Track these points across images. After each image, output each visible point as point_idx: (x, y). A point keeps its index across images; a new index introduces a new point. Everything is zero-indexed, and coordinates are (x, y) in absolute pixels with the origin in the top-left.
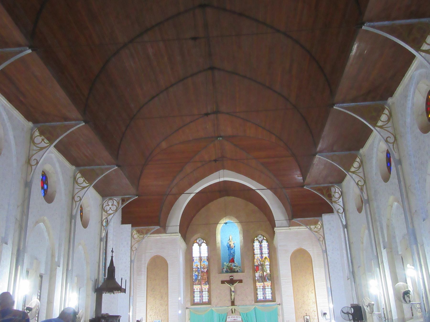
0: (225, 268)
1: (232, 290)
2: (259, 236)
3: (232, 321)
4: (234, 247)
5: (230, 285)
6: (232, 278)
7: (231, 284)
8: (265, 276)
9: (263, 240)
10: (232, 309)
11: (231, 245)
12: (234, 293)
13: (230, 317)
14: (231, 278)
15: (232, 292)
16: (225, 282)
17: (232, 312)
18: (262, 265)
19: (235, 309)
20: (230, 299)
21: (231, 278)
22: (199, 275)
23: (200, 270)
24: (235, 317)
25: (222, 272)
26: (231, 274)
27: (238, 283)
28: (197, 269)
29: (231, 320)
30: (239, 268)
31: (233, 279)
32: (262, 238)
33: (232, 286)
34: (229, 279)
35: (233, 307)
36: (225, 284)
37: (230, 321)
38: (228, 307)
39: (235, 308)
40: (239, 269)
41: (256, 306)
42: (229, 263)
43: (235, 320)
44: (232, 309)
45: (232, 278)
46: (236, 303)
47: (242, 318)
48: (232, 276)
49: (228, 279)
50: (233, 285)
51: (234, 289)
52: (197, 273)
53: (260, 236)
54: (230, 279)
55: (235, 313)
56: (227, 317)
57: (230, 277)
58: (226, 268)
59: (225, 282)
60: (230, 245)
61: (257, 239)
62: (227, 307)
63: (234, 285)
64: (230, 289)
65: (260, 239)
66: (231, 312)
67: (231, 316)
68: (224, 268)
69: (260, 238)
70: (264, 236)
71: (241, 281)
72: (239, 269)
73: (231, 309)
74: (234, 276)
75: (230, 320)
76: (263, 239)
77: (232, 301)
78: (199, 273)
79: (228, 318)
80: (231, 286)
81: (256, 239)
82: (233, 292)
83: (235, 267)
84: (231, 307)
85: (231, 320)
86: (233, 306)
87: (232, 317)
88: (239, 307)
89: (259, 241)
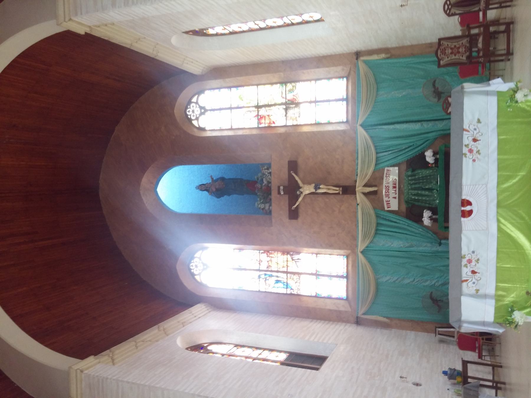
0: (263, 207)
1: (314, 191)
2: (190, 115)
3: (397, 196)
4: (222, 179)
5: (299, 196)
6: (282, 188)
7: (298, 192)
8: (284, 101)
9: (199, 105)
10: (365, 194)
11: (217, 187)
12: (321, 184)
13: (385, 199)
14: (282, 193)
15: (320, 191)
16: (293, 209)
17: (375, 193)
18: (258, 107)
19: (366, 185)
20: (338, 197)
21: (282, 193)
22: (277, 277)
23: (264, 273)
24: (387, 185)
25: (270, 213)
26: (274, 193)
27: (296, 174)
28: (262, 281)
29: (395, 198)
30: (264, 168)
31: (285, 187)
32: (193, 106)
33: (301, 190)
34: (287, 197)
35: (359, 189)
36: (300, 211)
37: (397, 200)
38: (358, 204)
39: (364, 183)
40: (265, 169)
41: (360, 122)
42: (256, 194)
43: (395, 187)
44: (365, 194)
45: (282, 188)
46: (347, 183)
47: (391, 166)
48: (279, 187)
49: (285, 201)
50: (300, 188)
51: (309, 183)
52: (272, 280)
53: (189, 111)
54: (284, 194)
55: (375, 186)
56: (386, 209)
57: (279, 193)
58: (262, 203)
59: (293, 209)
60: (217, 190)
61: (197, 119)
62: (359, 208)
63: (301, 184)
64: (323, 196)
65: (197, 111)
66: (372, 197)
67: (384, 196)
68: (263, 209)
69: (193, 111)
70: (190, 102)
71: (293, 166)
72: (265, 169)
73: (362, 196)
74: (279, 185)
75: (394, 199)
76: (197, 103)
77: (341, 194)
78: (271, 276)
79: (388, 208)
80: (302, 193)
81: (195, 123)
82: (317, 188)
83: (264, 179)
84: (359, 197)
85: (395, 198)
86: (357, 189)
87: (388, 196)
88: (359, 175)
89: (202, 114)
